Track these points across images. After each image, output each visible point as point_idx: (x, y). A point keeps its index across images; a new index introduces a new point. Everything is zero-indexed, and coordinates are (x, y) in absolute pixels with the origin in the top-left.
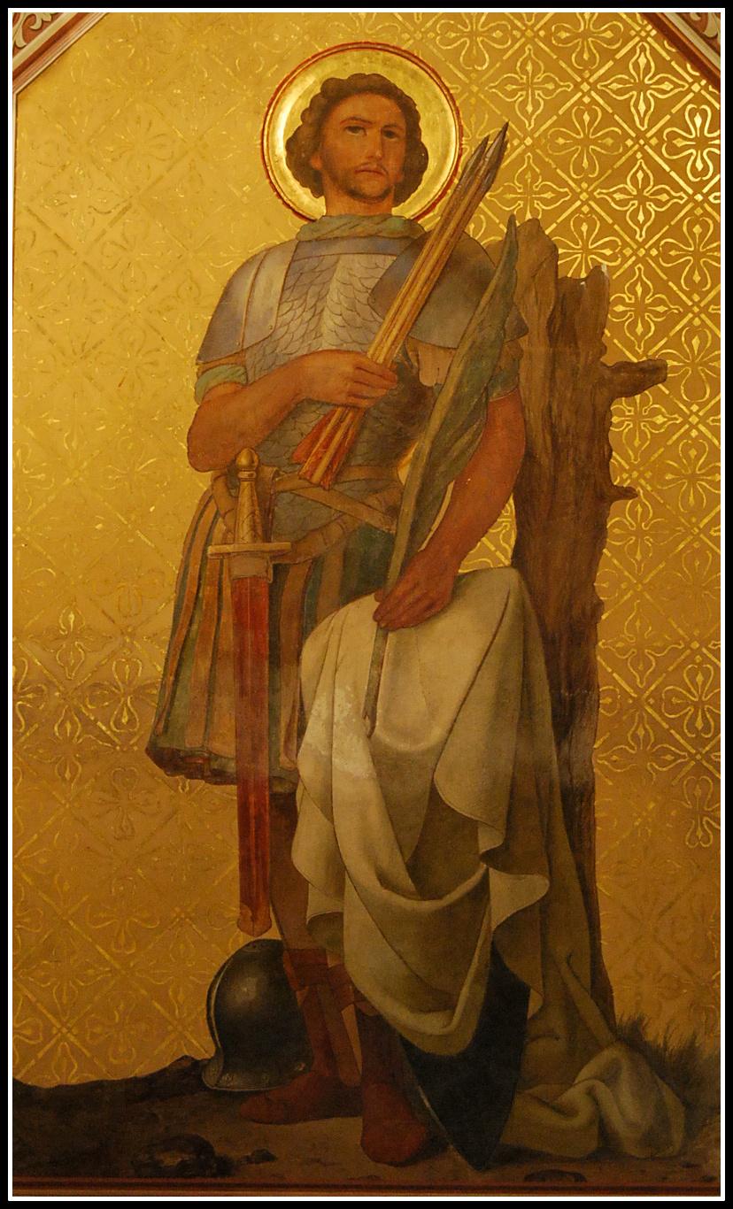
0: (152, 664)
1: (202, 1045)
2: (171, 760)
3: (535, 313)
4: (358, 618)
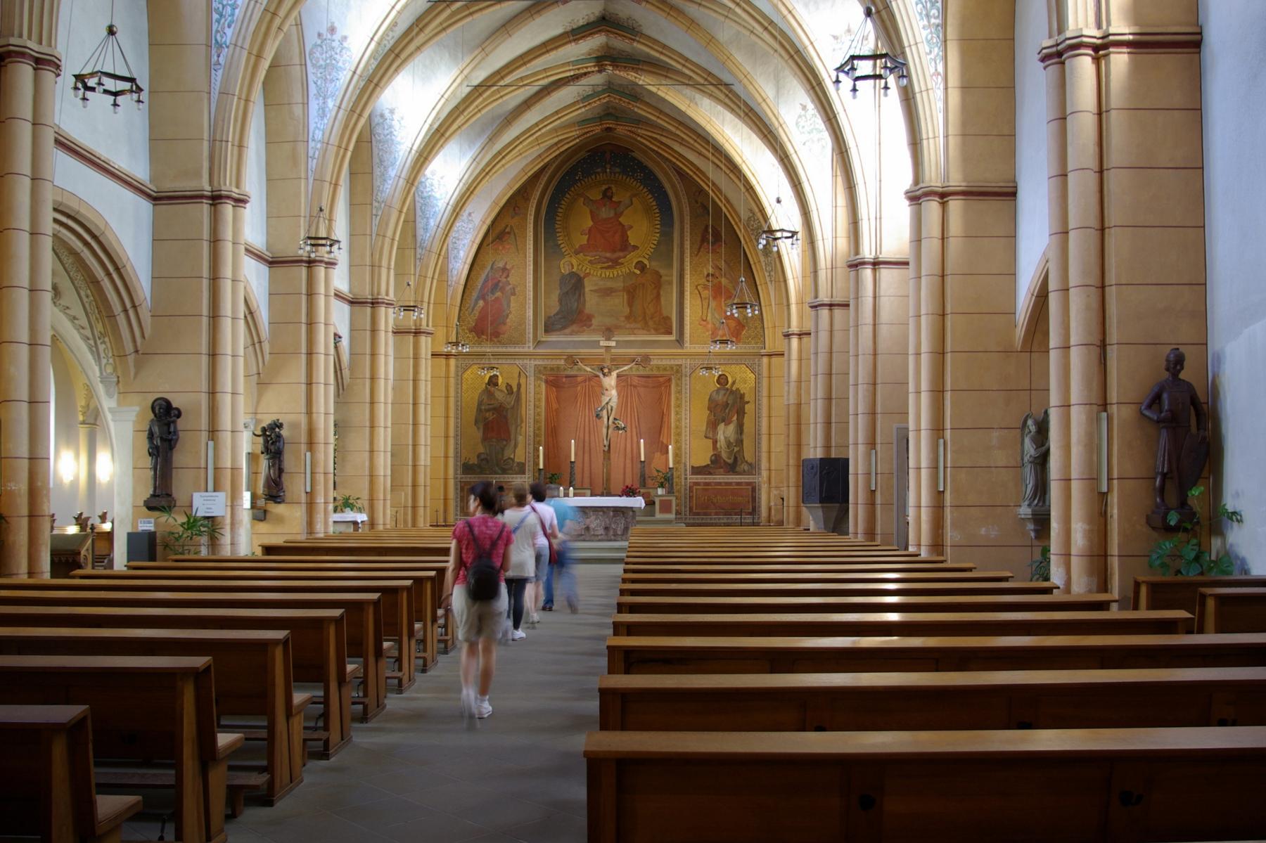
0: (704, 428)
1: (709, 463)
2: (706, 437)
3: (738, 396)
4: (723, 424)
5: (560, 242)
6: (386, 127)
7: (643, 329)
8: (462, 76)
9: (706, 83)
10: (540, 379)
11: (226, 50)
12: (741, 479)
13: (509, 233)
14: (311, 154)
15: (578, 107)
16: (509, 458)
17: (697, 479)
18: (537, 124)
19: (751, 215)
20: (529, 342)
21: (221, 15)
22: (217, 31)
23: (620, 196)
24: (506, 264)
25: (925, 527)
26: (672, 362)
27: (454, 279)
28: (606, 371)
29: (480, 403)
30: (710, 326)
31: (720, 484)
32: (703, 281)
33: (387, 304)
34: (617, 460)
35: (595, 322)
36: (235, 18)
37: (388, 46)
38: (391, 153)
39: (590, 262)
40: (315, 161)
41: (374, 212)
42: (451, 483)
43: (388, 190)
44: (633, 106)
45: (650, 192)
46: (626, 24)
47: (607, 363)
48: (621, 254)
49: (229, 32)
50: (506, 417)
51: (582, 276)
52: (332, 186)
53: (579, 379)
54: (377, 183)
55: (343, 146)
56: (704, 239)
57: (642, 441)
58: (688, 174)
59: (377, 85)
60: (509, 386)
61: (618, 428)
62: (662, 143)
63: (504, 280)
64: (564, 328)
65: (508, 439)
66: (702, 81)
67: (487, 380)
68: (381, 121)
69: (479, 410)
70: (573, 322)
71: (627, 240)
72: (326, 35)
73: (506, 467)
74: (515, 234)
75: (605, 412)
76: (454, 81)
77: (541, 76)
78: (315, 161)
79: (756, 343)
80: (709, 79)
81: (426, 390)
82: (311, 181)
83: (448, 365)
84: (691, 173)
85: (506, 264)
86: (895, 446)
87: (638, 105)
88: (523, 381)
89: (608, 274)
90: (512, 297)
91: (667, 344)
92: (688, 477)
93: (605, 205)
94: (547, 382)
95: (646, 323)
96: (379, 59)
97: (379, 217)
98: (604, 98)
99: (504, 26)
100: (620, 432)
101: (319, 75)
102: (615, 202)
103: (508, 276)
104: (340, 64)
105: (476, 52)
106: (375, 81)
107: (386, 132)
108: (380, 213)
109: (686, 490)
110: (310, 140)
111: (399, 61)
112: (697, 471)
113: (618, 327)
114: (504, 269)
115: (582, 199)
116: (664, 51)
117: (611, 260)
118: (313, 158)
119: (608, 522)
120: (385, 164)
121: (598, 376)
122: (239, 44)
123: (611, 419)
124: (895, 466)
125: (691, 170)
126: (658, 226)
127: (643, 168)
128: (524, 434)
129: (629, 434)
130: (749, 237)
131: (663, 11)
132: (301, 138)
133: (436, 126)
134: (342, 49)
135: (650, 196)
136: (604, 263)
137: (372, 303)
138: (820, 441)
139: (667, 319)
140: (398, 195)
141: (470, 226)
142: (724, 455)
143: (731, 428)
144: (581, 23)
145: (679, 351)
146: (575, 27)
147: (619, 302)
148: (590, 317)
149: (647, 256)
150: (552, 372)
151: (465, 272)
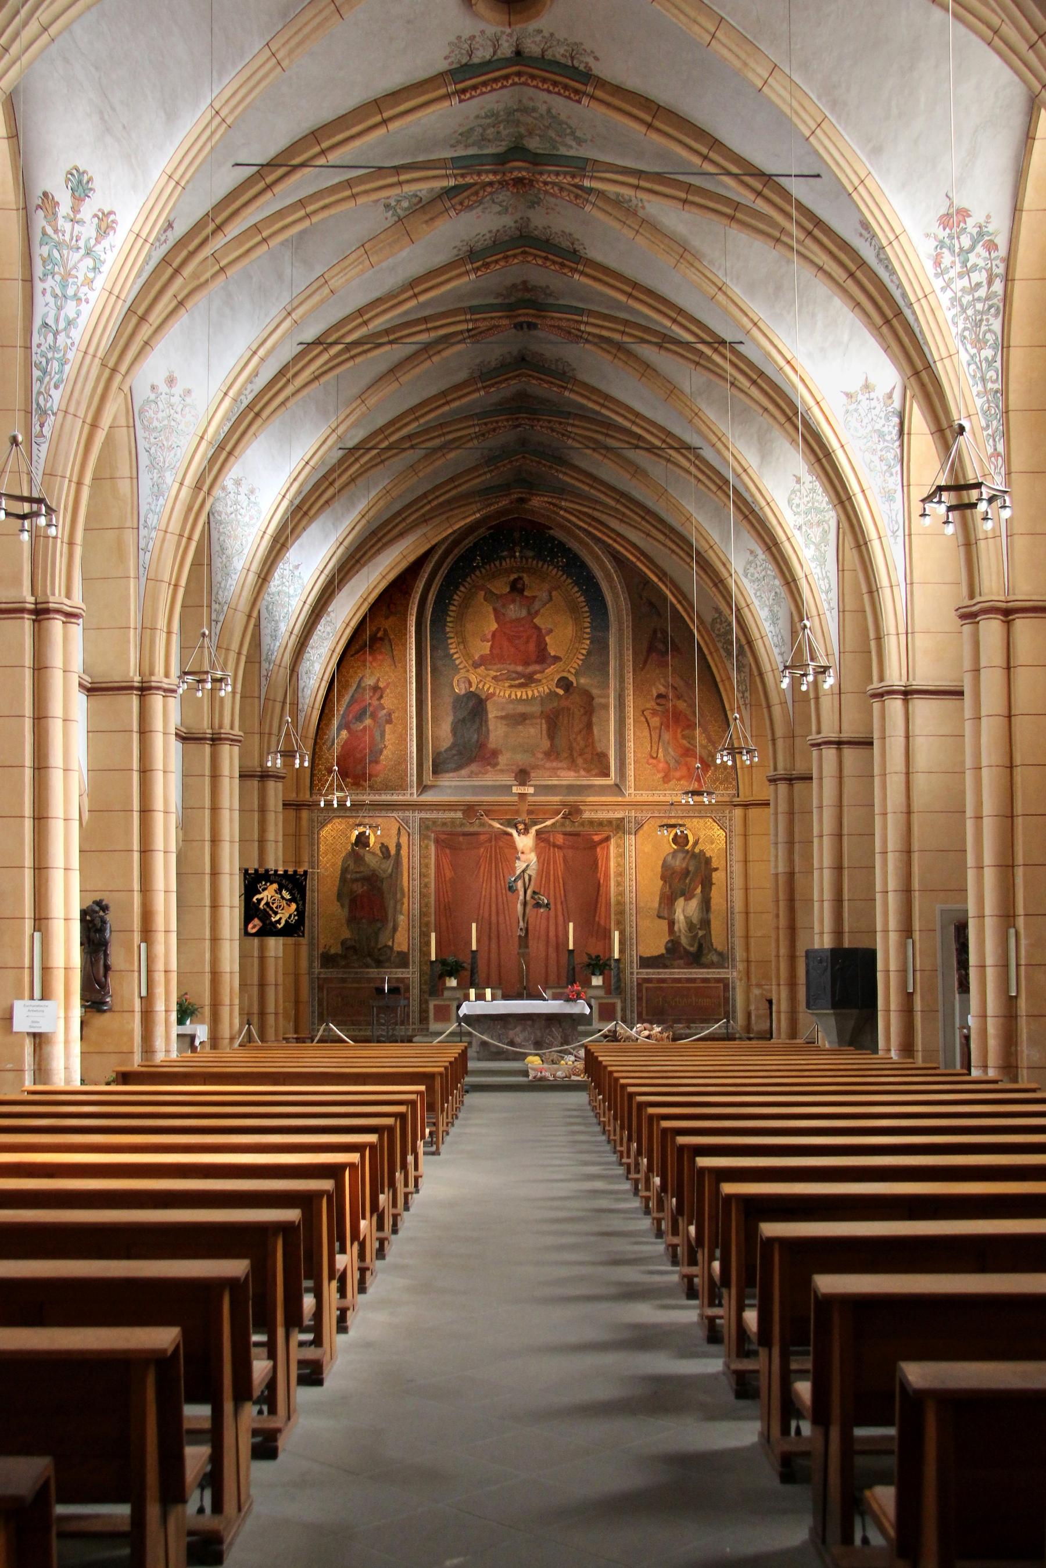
0: (656, 905)
1: (663, 951)
2: (659, 917)
5: (452, 651)
6: (229, 503)
7: (569, 769)
8: (334, 437)
9: (664, 446)
10: (427, 837)
11: (53, 418)
12: (708, 973)
13: (381, 639)
14: (142, 545)
15: (481, 472)
16: (386, 946)
17: (647, 974)
18: (425, 495)
19: (717, 615)
20: (411, 787)
21: (45, 372)
22: (39, 393)
23: (537, 589)
24: (378, 680)
25: (993, 1043)
26: (611, 815)
27: (307, 701)
28: (521, 827)
29: (344, 871)
30: (661, 765)
31: (679, 980)
32: (652, 704)
33: (232, 740)
34: (536, 947)
35: (502, 760)
36: (65, 377)
37: (246, 403)
38: (236, 537)
39: (495, 678)
40: (148, 555)
41: (214, 617)
42: (305, 981)
43: (232, 588)
44: (557, 471)
45: (576, 583)
46: (553, 367)
47: (524, 817)
48: (537, 667)
49: (56, 394)
50: (380, 890)
51: (483, 697)
52: (172, 587)
53: (482, 838)
54: (217, 578)
55: (186, 534)
56: (651, 649)
57: (571, 925)
58: (628, 559)
59: (230, 453)
60: (384, 848)
61: (538, 905)
62: (594, 519)
63: (375, 702)
64: (459, 768)
65: (384, 920)
66: (658, 443)
67: (353, 839)
68: (223, 495)
69: (343, 879)
70: (471, 760)
71: (545, 649)
72: (163, 388)
73: (381, 957)
74: (390, 640)
75: (520, 884)
76: (324, 442)
77: (436, 434)
78: (148, 555)
79: (726, 789)
80: (668, 440)
81: (276, 854)
82: (143, 580)
83: (298, 819)
84: (634, 560)
85: (378, 680)
86: (938, 933)
87: (564, 470)
88: (404, 840)
89: (519, 695)
90: (388, 727)
91: (603, 790)
92: (635, 970)
93: (513, 601)
94: (437, 841)
95: (573, 761)
96: (233, 420)
97: (220, 624)
98: (517, 460)
99: (392, 371)
100: (542, 910)
101: (152, 440)
102: (527, 597)
103: (381, 697)
104: (182, 427)
105: (354, 405)
106: (228, 448)
107: (229, 510)
108: (221, 618)
109: (632, 988)
110: (141, 527)
111: (259, 421)
112: (646, 962)
113: (536, 767)
114: (376, 688)
115: (482, 593)
116: (607, 403)
117: (521, 675)
118: (145, 550)
119: (539, 1034)
120: (229, 552)
121: (511, 835)
122: (72, 410)
123: (529, 892)
124: (939, 961)
125: (632, 554)
126: (588, 630)
127: (566, 551)
128: (406, 913)
129: (552, 913)
130: (715, 646)
131: (609, 352)
132: (128, 524)
133: (297, 502)
134: (185, 406)
135: (576, 589)
136: (514, 679)
137: (212, 740)
138: (828, 925)
139: (603, 757)
140: (247, 594)
141: (329, 629)
142: (684, 941)
143: (694, 904)
144: (493, 364)
145: (620, 799)
146: (485, 370)
147: (535, 733)
148: (495, 753)
149: (573, 671)
150: (444, 829)
151: (322, 692)
